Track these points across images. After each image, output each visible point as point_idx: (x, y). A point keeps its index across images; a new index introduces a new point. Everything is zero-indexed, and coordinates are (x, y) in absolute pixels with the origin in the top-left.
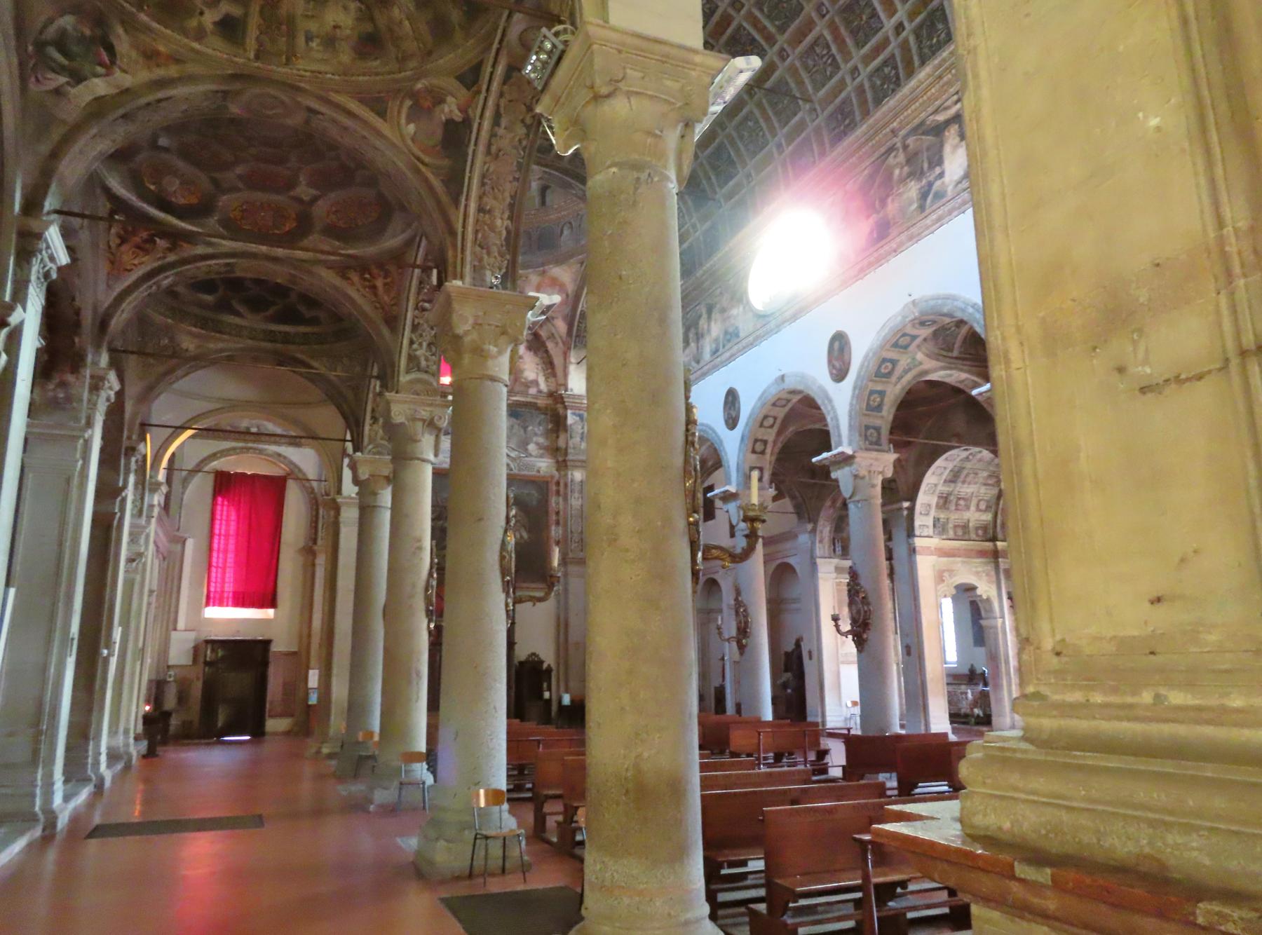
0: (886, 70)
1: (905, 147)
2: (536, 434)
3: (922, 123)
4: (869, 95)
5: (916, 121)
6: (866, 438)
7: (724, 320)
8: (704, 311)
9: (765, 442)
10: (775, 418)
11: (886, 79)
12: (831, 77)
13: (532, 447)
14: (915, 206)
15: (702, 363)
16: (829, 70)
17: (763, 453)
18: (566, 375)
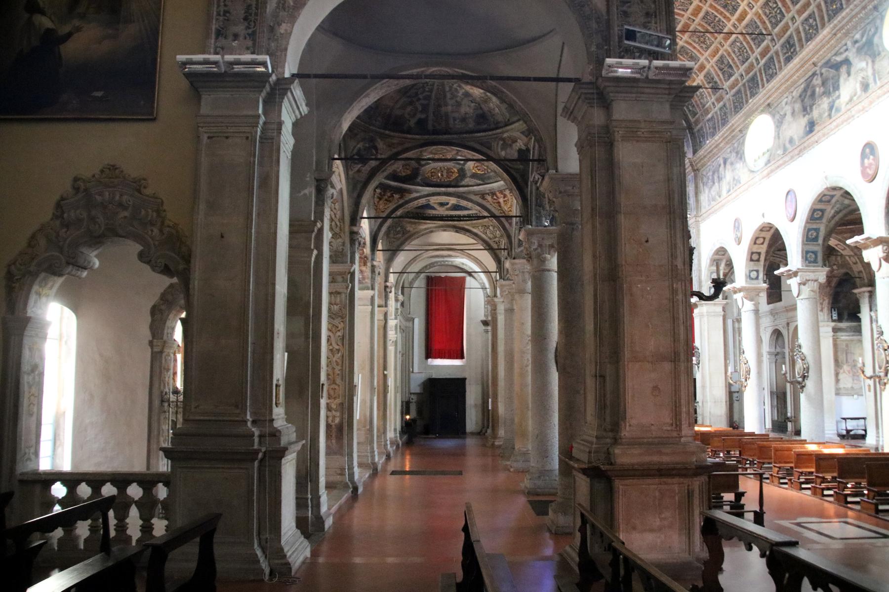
0: (811, 21)
1: (822, 74)
3: (830, 60)
4: (803, 35)
5: (827, 58)
6: (806, 259)
7: (733, 170)
8: (722, 162)
9: (759, 254)
10: (764, 238)
11: (811, 26)
12: (781, 21)
14: (826, 114)
15: (722, 197)
16: (779, 16)
17: (758, 260)
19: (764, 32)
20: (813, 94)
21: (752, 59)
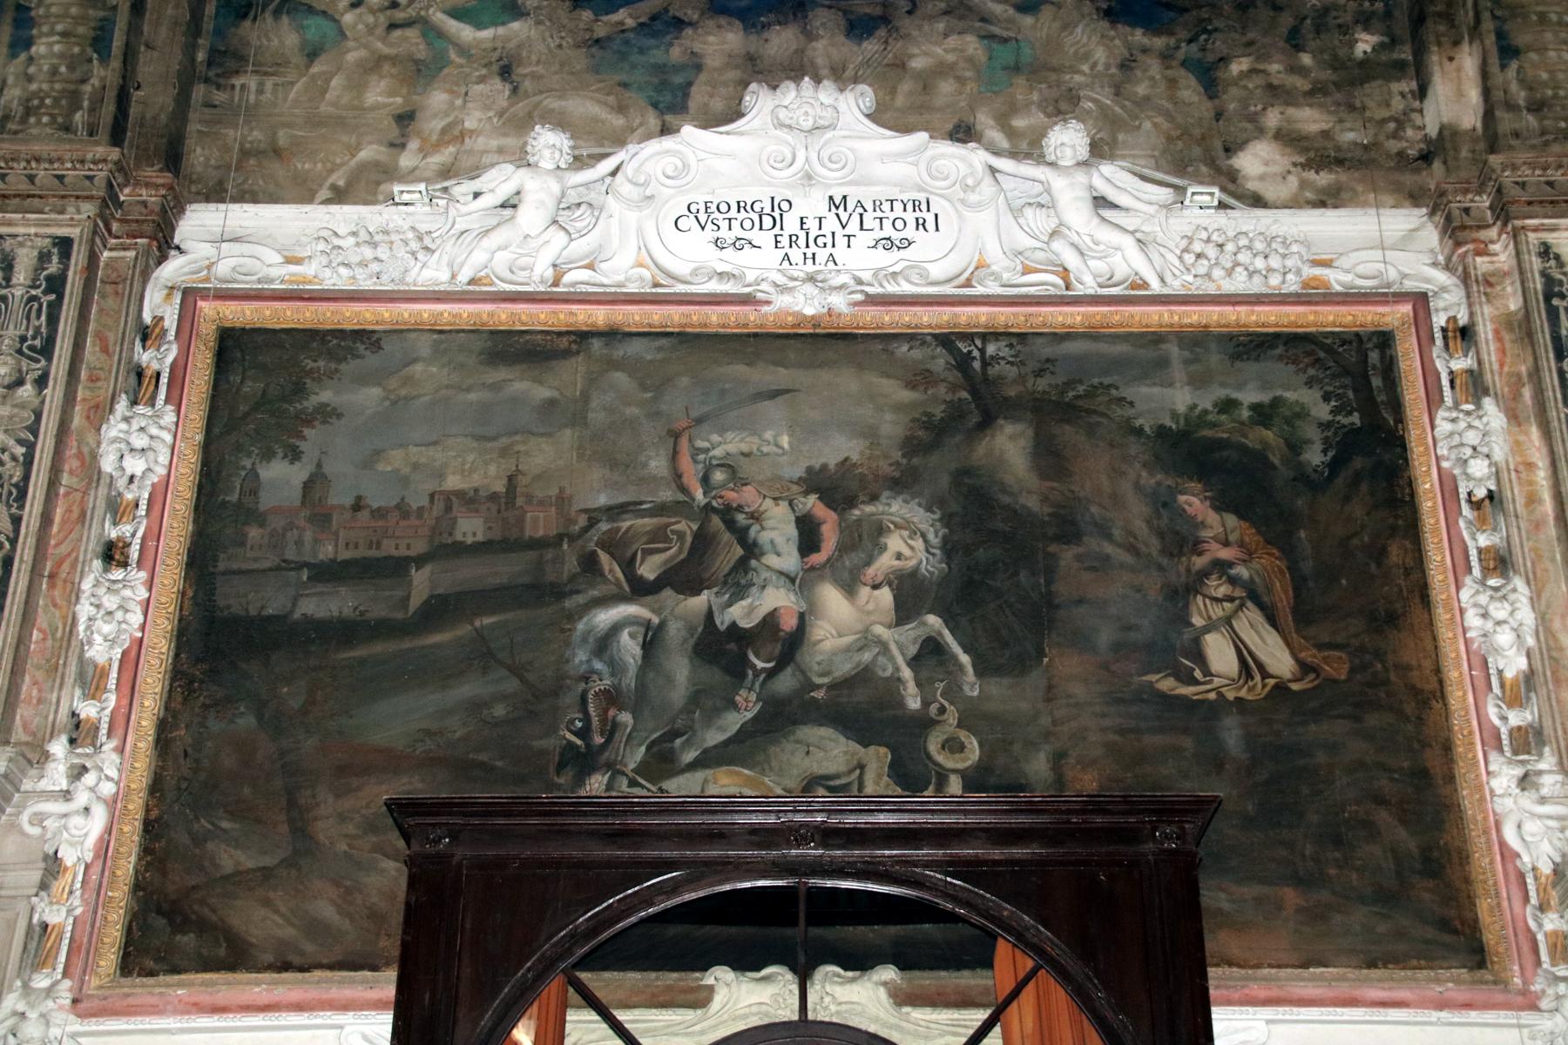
2: (1276, 93)
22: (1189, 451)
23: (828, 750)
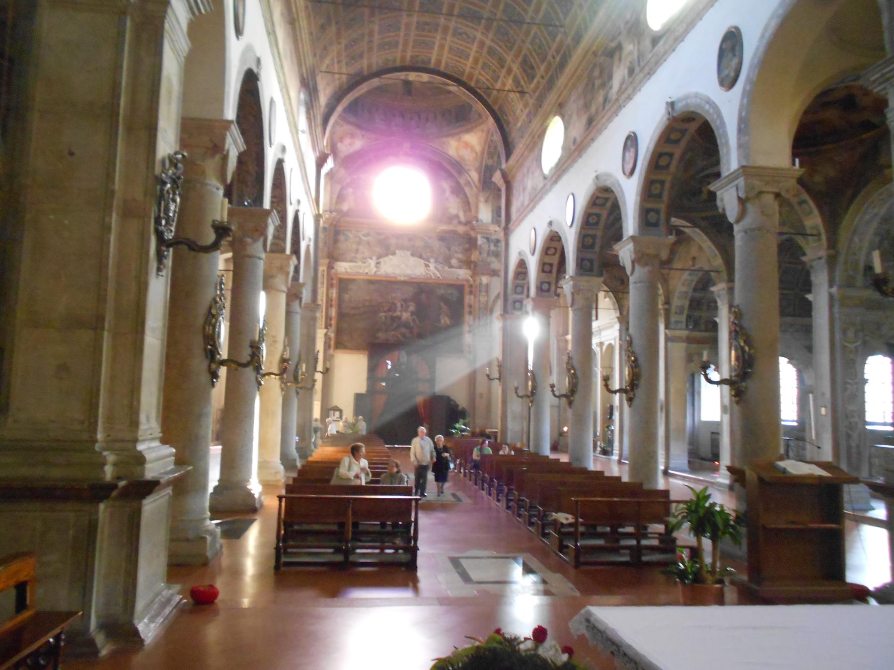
2: (456, 252)
9: (551, 265)
10: (556, 249)
13: (454, 262)
17: (550, 272)
18: (477, 208)
19: (557, 24)
20: (593, 85)
21: (550, 57)
22: (442, 298)
23: (404, 330)
